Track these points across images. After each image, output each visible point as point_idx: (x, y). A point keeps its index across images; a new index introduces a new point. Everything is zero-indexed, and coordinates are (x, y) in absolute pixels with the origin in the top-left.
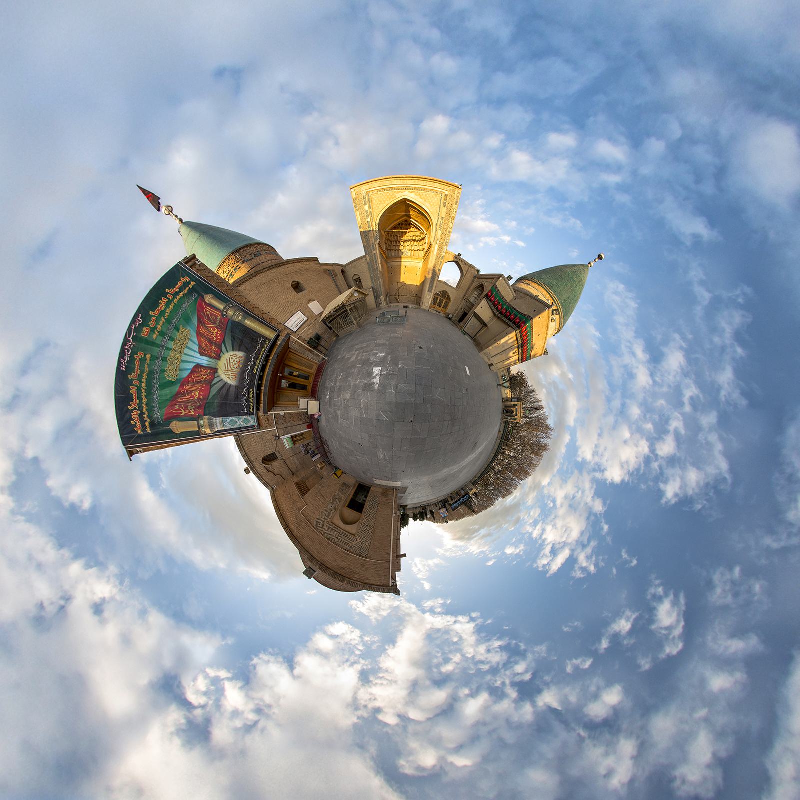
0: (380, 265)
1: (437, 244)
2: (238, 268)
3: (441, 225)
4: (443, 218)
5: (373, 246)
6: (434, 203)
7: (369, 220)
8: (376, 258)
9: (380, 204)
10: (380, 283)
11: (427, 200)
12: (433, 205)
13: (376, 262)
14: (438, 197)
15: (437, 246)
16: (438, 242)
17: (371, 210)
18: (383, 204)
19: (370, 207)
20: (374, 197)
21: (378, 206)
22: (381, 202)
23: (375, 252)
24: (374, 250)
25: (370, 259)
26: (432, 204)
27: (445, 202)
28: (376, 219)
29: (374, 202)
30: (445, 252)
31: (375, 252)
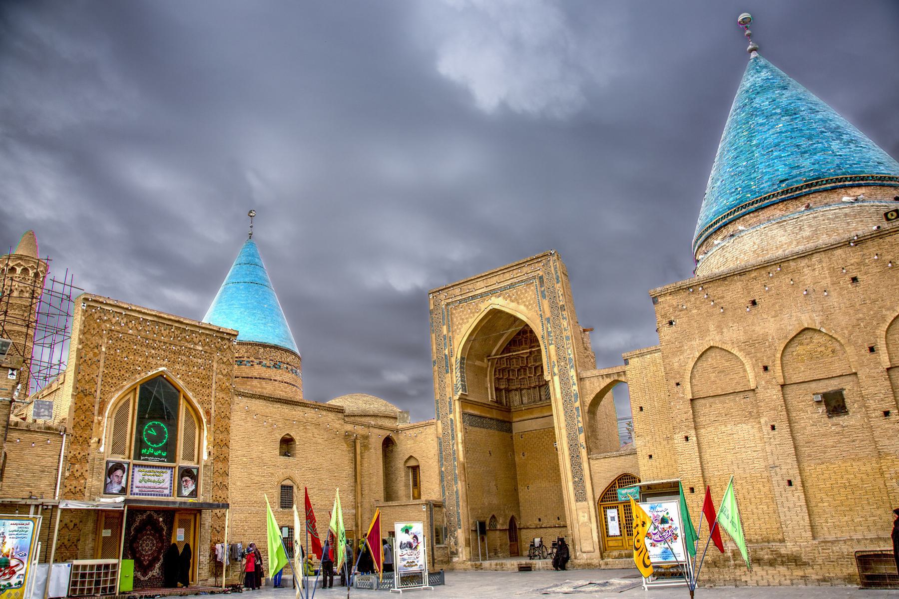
0: (460, 447)
1: (555, 375)
2: (252, 363)
3: (549, 333)
4: (549, 322)
5: (450, 402)
6: (530, 301)
8: (452, 430)
9: (461, 324)
10: (457, 492)
11: (520, 301)
12: (530, 304)
13: (453, 438)
14: (532, 288)
15: (556, 379)
16: (556, 370)
17: (450, 334)
18: (465, 323)
19: (448, 331)
20: (454, 312)
21: (460, 326)
22: (463, 319)
23: (451, 416)
24: (450, 412)
25: (443, 429)
26: (527, 303)
27: (543, 289)
28: (456, 350)
29: (455, 320)
30: (575, 381)
31: (451, 416)
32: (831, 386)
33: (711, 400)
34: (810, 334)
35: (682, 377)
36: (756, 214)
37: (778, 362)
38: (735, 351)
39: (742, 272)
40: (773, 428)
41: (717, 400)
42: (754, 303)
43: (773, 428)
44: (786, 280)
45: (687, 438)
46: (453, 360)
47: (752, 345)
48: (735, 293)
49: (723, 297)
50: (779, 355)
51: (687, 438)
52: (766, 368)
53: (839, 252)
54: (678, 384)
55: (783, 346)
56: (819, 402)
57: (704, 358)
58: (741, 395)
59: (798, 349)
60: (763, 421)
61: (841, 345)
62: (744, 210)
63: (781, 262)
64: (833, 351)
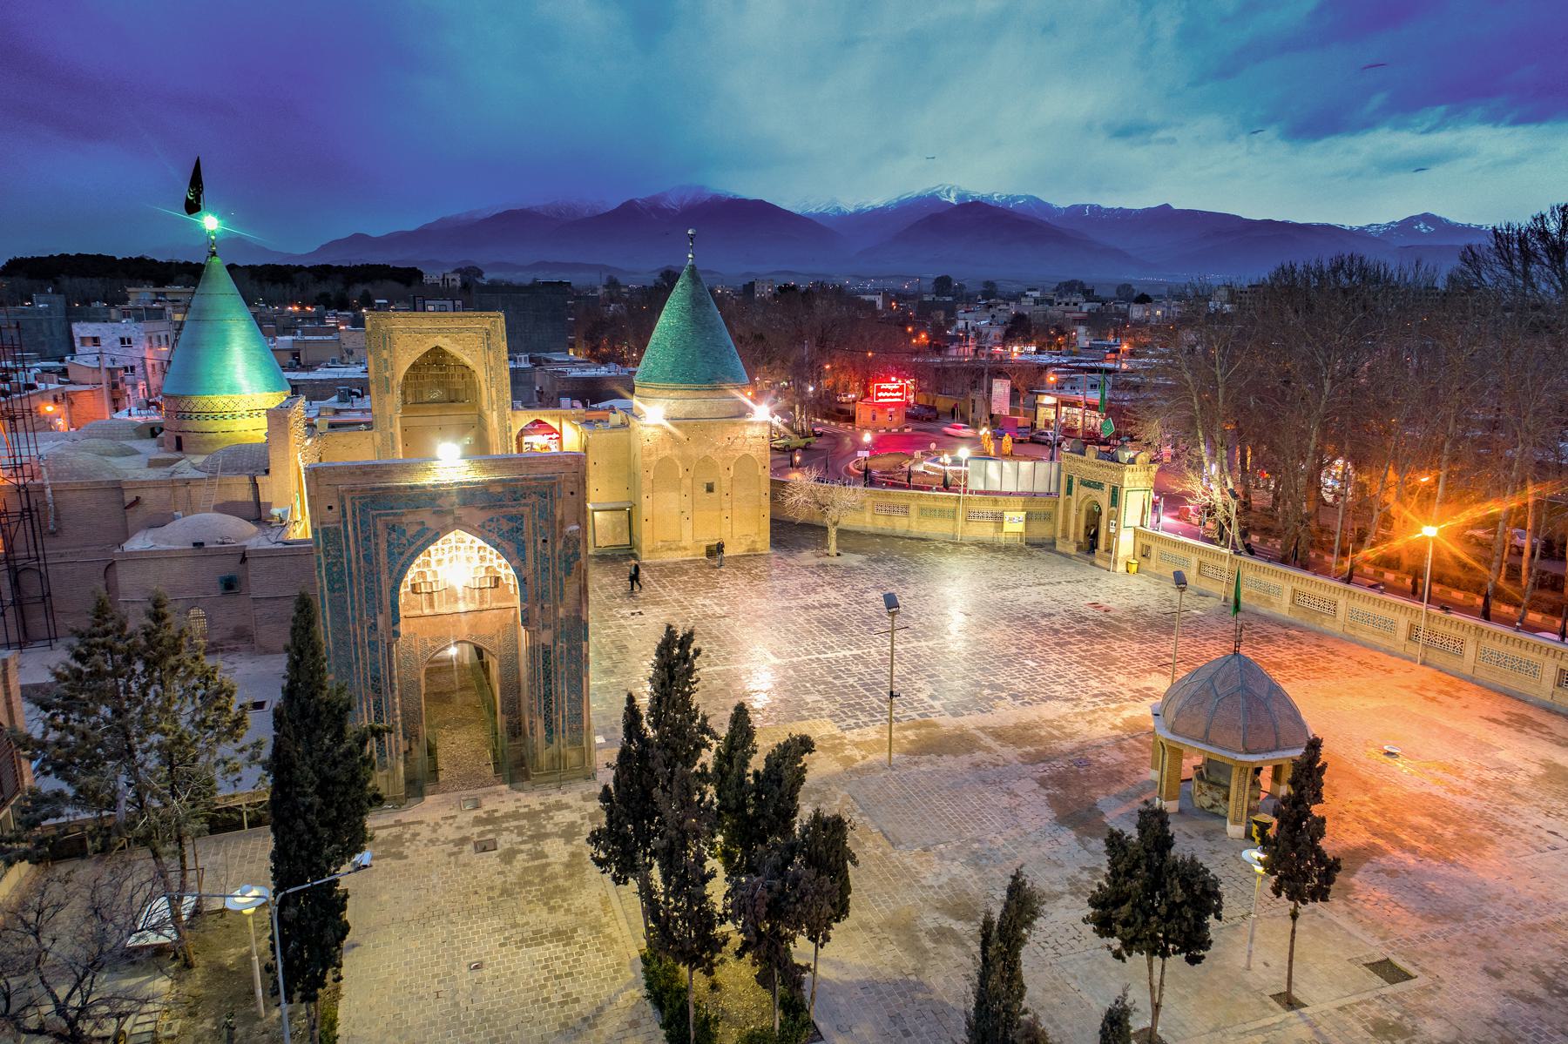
7: (387, 374)
13: (393, 448)
46: (395, 383)
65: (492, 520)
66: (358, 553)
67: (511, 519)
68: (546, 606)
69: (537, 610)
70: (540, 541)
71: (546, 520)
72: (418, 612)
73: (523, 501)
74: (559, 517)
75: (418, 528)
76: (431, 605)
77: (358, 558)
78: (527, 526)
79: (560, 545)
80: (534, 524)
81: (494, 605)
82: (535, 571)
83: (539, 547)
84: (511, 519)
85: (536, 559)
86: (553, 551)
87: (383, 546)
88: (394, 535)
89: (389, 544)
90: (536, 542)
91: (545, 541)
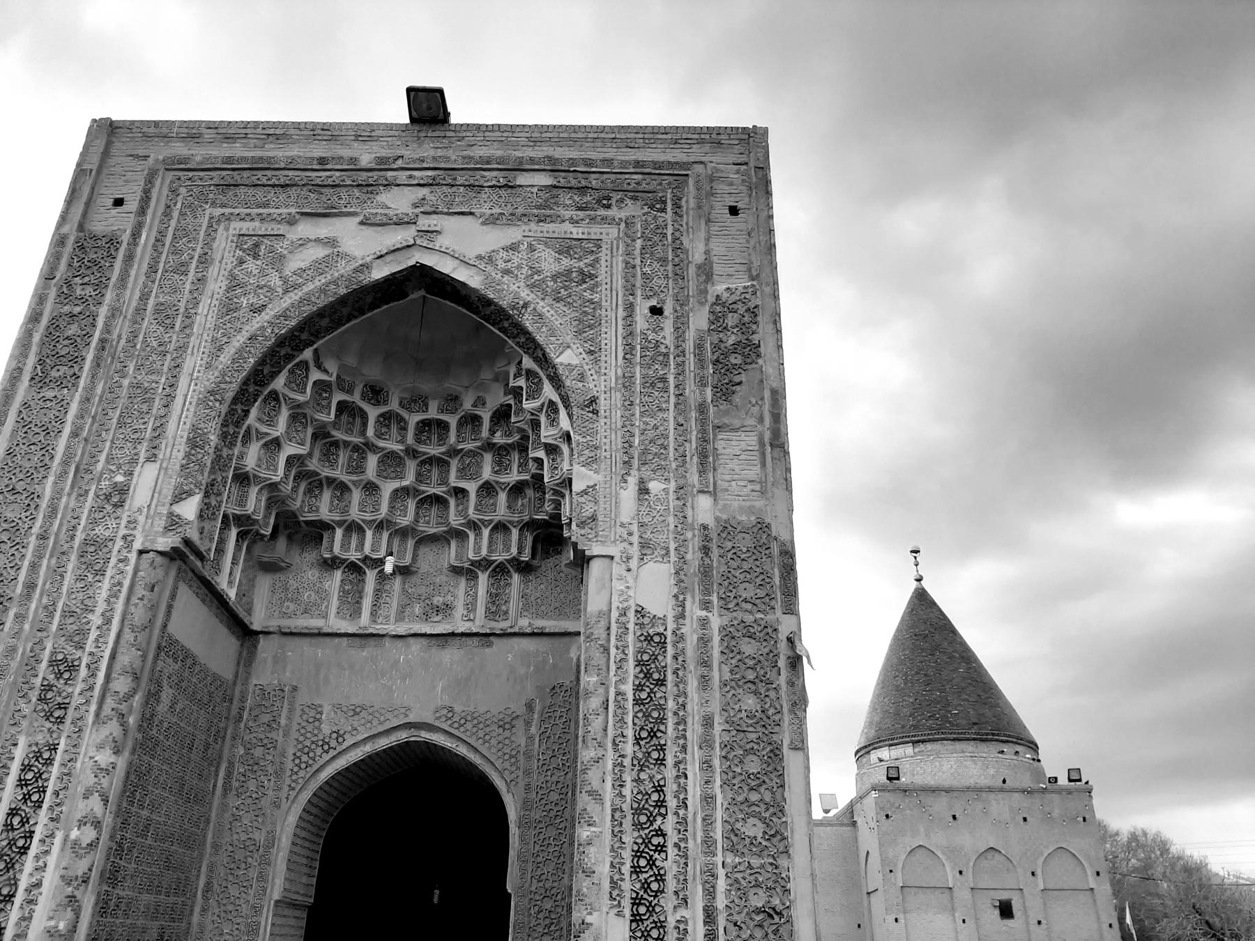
32: (1004, 896)
33: (916, 890)
34: (992, 852)
35: (895, 865)
36: (952, 742)
37: (971, 870)
38: (939, 854)
39: (948, 791)
40: (964, 921)
41: (920, 891)
42: (954, 817)
43: (964, 921)
44: (979, 806)
45: (896, 920)
47: (952, 852)
48: (940, 805)
49: (931, 806)
50: (971, 864)
51: (896, 920)
52: (961, 872)
53: (1016, 795)
54: (891, 871)
55: (975, 857)
56: (995, 906)
57: (912, 854)
58: (940, 891)
59: (984, 863)
60: (957, 915)
61: (1014, 866)
62: (943, 736)
63: (978, 790)
64: (1008, 870)
65: (513, 247)
66: (144, 297)
67: (566, 247)
68: (655, 486)
69: (628, 495)
70: (642, 308)
71: (663, 261)
72: (315, 623)
73: (602, 212)
74: (698, 256)
75: (327, 251)
76: (356, 613)
77: (140, 310)
78: (611, 270)
79: (699, 320)
80: (629, 266)
81: (524, 624)
82: (627, 382)
83: (642, 320)
84: (566, 247)
85: (629, 349)
86: (680, 335)
87: (216, 284)
88: (252, 265)
89: (234, 284)
90: (630, 308)
91: (656, 311)
